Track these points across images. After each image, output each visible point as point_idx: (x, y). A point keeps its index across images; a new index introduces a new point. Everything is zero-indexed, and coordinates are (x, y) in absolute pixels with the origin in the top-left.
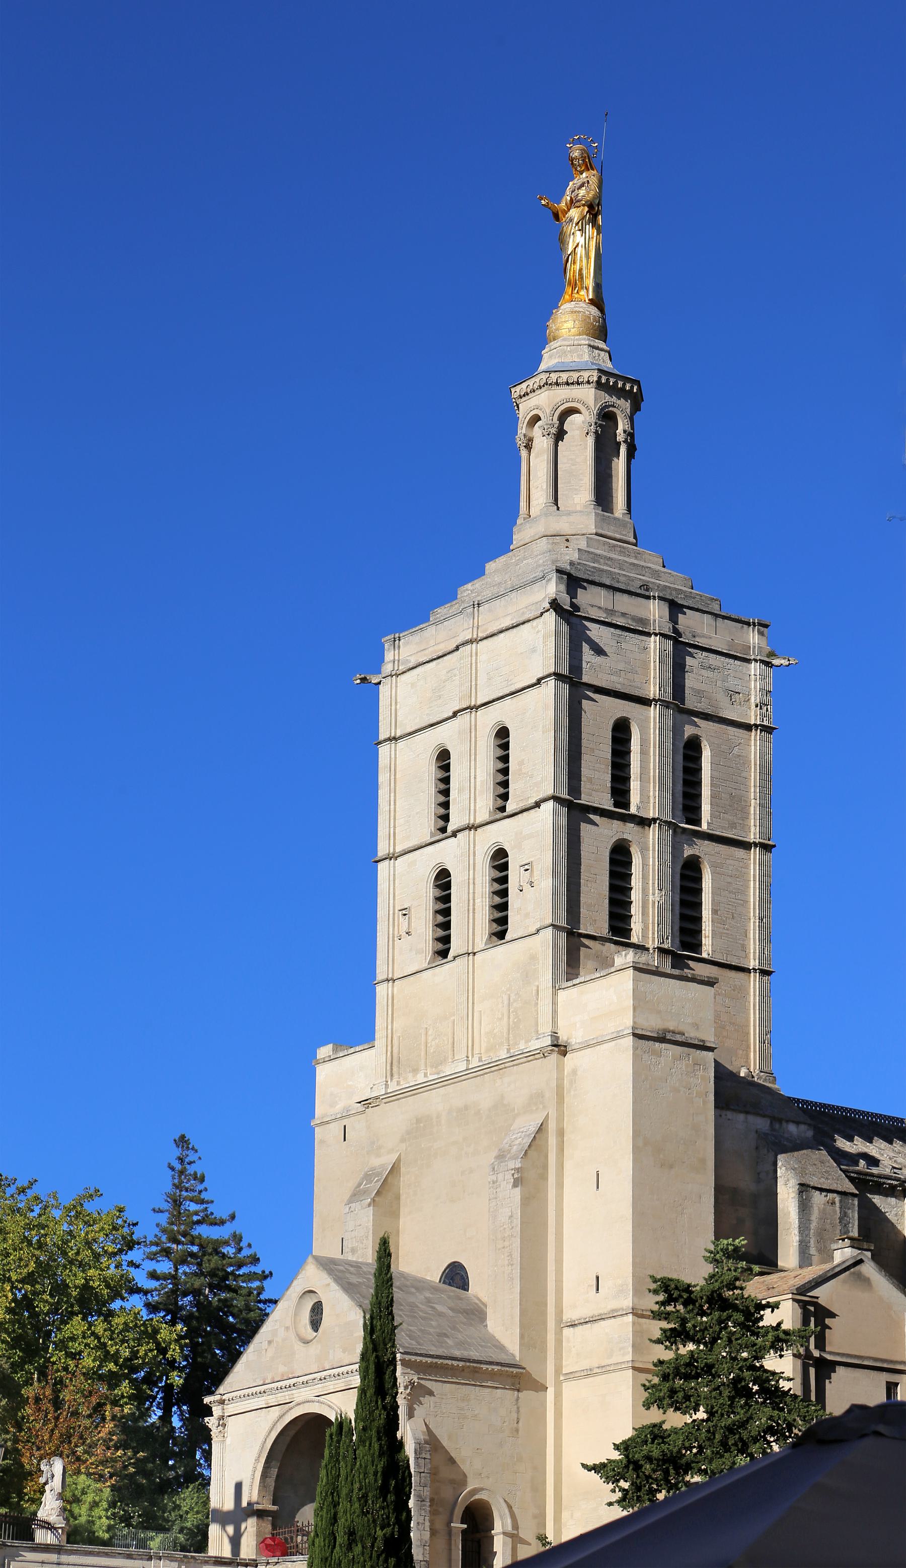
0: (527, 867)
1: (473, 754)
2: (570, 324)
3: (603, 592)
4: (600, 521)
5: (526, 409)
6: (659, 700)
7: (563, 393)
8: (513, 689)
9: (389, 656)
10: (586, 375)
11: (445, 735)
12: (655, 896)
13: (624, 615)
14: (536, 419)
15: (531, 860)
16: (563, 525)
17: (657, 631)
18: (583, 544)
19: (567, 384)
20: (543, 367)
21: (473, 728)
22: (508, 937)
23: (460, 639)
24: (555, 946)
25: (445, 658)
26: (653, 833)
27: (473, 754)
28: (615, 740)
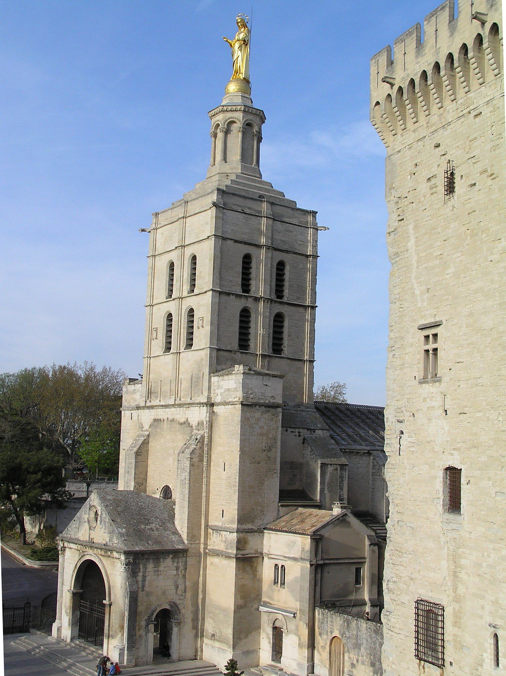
0: (202, 319)
1: (182, 266)
2: (234, 87)
3: (241, 199)
4: (243, 168)
6: (265, 245)
8: (198, 240)
10: (239, 108)
13: (249, 208)
15: (203, 316)
16: (227, 168)
17: (265, 216)
18: (234, 178)
19: (231, 111)
21: (183, 255)
22: (193, 348)
24: (211, 357)
25: (174, 223)
27: (182, 266)
28: (244, 262)
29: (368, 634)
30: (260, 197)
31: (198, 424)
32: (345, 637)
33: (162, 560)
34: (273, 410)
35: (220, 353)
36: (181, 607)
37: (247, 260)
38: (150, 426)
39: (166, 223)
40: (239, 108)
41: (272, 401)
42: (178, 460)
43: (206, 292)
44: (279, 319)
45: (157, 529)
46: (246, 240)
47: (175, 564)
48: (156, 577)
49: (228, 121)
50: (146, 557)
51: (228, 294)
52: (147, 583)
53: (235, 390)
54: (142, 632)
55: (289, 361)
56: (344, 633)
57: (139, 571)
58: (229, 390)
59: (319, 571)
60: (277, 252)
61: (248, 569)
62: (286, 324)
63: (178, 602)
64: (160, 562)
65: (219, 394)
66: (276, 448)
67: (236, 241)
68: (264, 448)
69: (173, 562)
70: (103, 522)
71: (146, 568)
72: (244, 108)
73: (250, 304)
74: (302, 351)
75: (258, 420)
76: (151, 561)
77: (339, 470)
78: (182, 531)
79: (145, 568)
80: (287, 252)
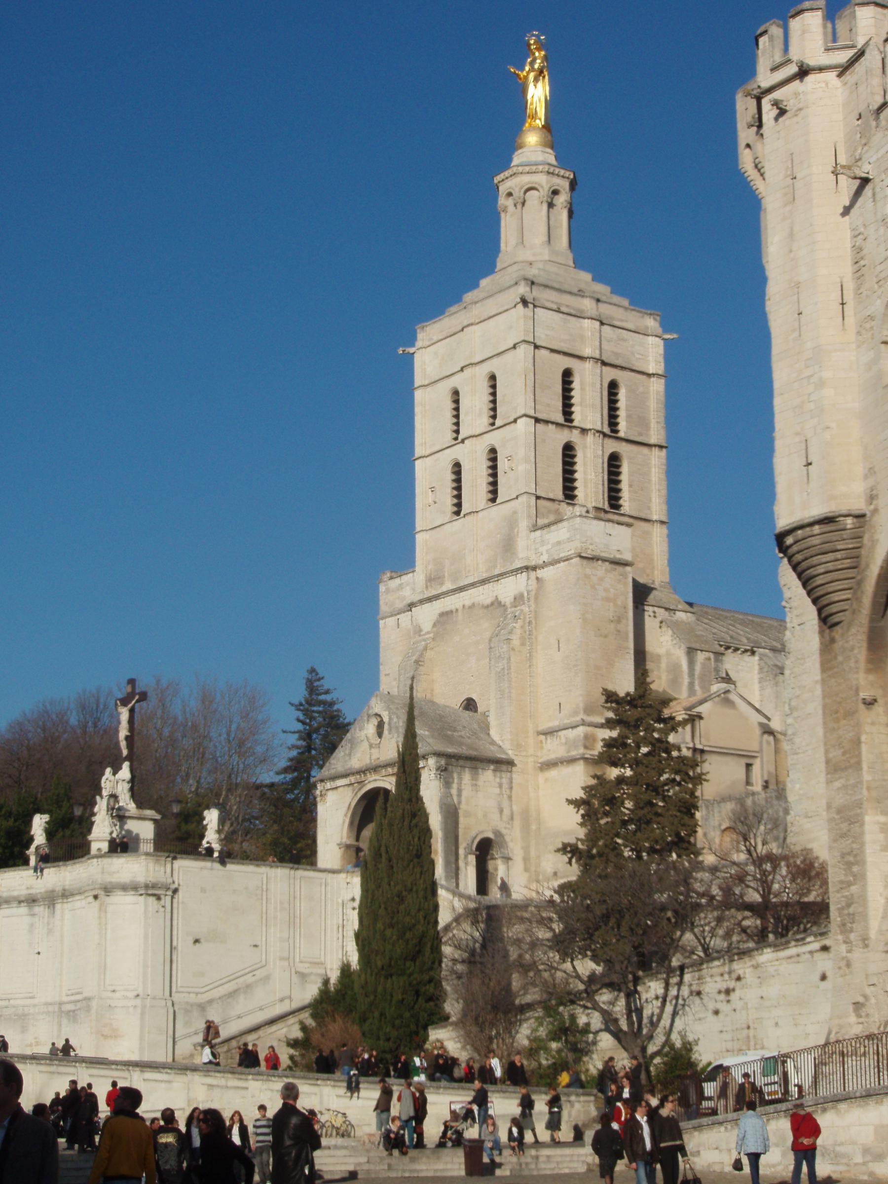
5: (503, 189)
11: (454, 382)
12: (591, 476)
13: (567, 306)
14: (510, 194)
18: (541, 265)
20: (512, 164)
22: (498, 501)
23: (465, 324)
26: (590, 438)
30: (579, 291)
31: (515, 599)
33: (480, 770)
34: (620, 569)
35: (539, 502)
36: (507, 838)
37: (567, 375)
38: (434, 625)
39: (440, 338)
40: (541, 168)
41: (618, 556)
42: (491, 648)
43: (515, 421)
44: (614, 461)
46: (566, 350)
47: (498, 780)
49: (526, 187)
51: (547, 422)
53: (570, 540)
57: (453, 782)
58: (559, 543)
62: (625, 469)
63: (504, 831)
64: (477, 774)
65: (544, 553)
66: (627, 620)
67: (553, 351)
68: (611, 618)
69: (495, 776)
70: (393, 731)
73: (574, 437)
74: (649, 508)
75: (601, 579)
76: (467, 769)
77: (713, 660)
78: (502, 741)
79: (460, 779)
80: (623, 368)
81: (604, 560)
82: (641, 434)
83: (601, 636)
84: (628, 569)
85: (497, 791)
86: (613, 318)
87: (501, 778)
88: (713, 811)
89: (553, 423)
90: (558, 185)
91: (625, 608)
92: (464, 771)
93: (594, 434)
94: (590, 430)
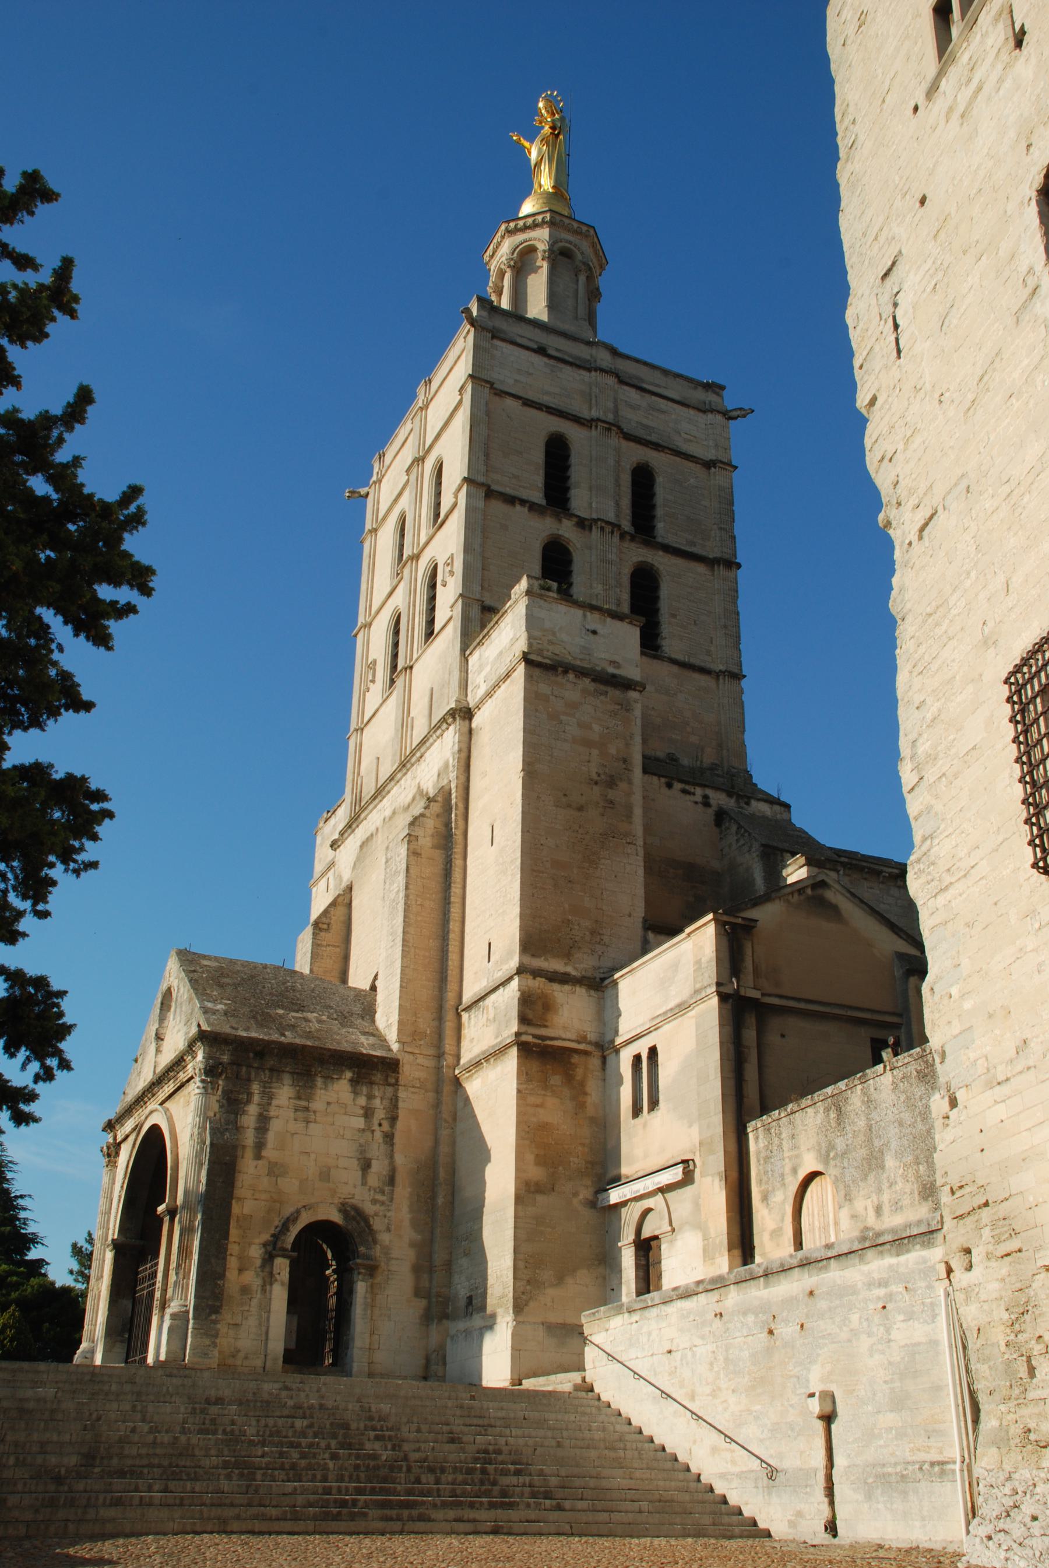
7: (520, 237)
9: (376, 470)
10: (540, 218)
13: (557, 350)
29: (903, 1097)
32: (834, 1158)
33: (319, 1081)
34: (615, 693)
36: (377, 1224)
41: (611, 670)
45: (320, 1021)
47: (362, 1101)
48: (300, 1126)
50: (271, 1062)
51: (511, 500)
52: (271, 1136)
54: (252, 1278)
55: (675, 669)
56: (831, 1147)
57: (249, 1101)
59: (751, 1020)
60: (632, 444)
61: (556, 1080)
63: (369, 1208)
64: (313, 1087)
67: (528, 403)
68: (595, 777)
69: (356, 1093)
71: (271, 1097)
72: (551, 217)
73: (567, 530)
76: (287, 1079)
79: (268, 1097)
80: (657, 446)
81: (582, 673)
82: (693, 544)
83: (569, 806)
84: (633, 695)
85: (360, 1123)
86: (642, 381)
87: (370, 1097)
88: (779, 1135)
89: (523, 502)
90: (570, 243)
91: (625, 761)
92: (280, 1080)
93: (602, 529)
94: (596, 521)
